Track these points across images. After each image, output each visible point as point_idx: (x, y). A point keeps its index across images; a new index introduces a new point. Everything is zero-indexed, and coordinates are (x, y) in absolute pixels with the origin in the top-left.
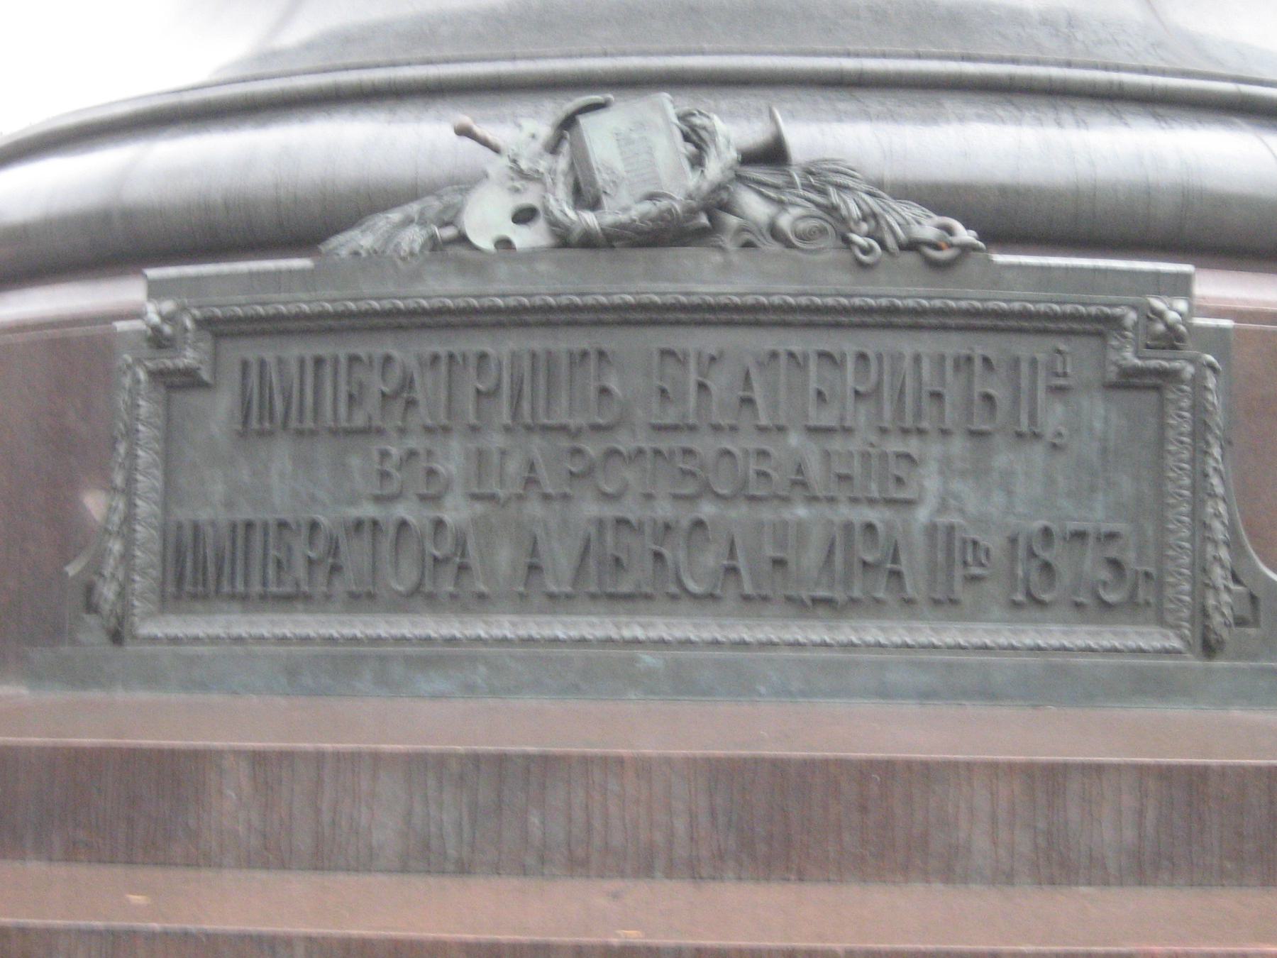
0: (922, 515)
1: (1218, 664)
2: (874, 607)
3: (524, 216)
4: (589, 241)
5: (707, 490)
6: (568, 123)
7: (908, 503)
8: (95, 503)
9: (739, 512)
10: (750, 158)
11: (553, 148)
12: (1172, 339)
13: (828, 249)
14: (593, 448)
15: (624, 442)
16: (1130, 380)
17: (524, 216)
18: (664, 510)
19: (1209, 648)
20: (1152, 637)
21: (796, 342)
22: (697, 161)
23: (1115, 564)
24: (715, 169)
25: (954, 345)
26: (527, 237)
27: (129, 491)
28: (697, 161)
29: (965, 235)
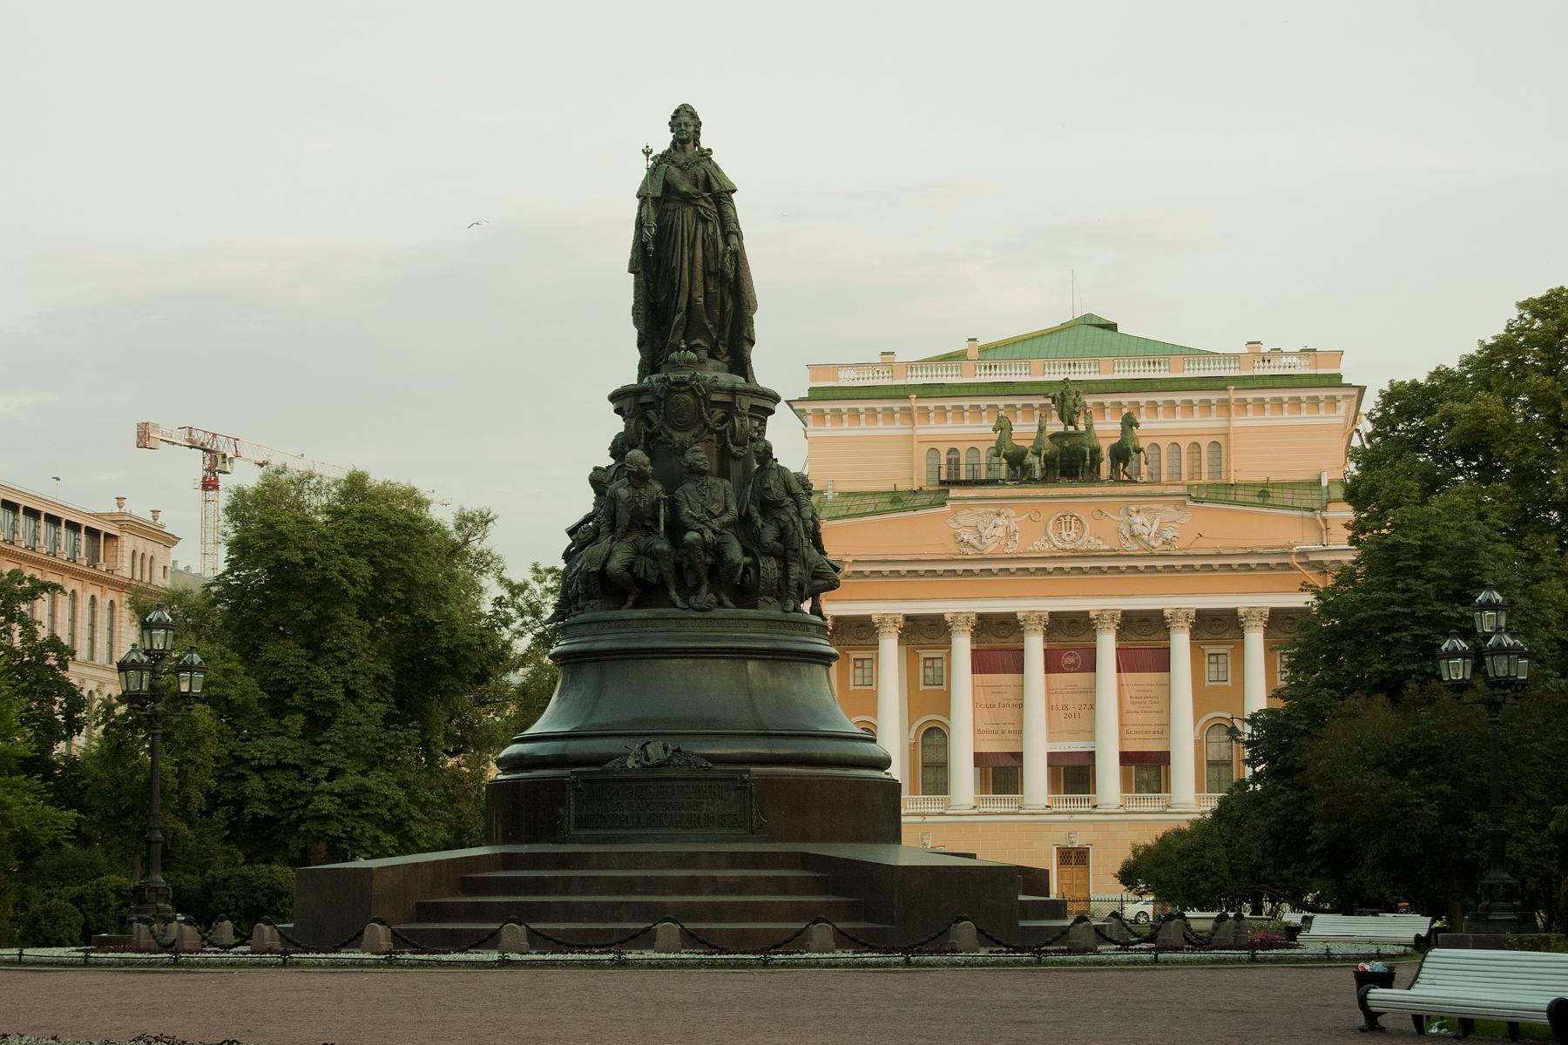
0: (704, 812)
1: (755, 836)
2: (696, 827)
3: (637, 762)
4: (647, 767)
5: (667, 808)
6: (644, 745)
7: (701, 810)
8: (561, 811)
9: (674, 812)
10: (674, 751)
11: (642, 749)
12: (746, 781)
13: (687, 768)
14: (649, 802)
15: (654, 801)
16: (738, 788)
17: (637, 762)
18: (661, 812)
19: (753, 833)
20: (741, 831)
21: (683, 784)
22: (666, 753)
23: (736, 819)
24: (668, 755)
25: (709, 783)
26: (637, 766)
27: (569, 808)
28: (666, 753)
29: (710, 765)
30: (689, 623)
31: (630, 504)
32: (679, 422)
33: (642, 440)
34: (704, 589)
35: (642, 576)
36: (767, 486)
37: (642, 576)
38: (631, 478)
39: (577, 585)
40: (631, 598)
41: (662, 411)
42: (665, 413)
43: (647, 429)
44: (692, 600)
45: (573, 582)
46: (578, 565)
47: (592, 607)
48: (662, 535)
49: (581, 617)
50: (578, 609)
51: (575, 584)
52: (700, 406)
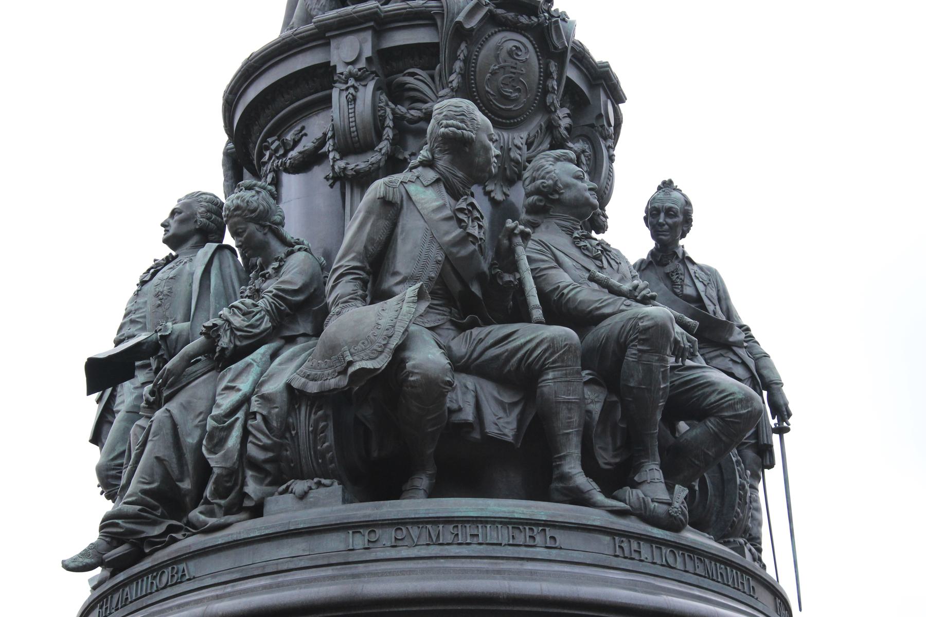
30: (646, 551)
31: (445, 226)
32: (507, 99)
33: (389, 133)
34: (653, 472)
35: (468, 415)
36: (689, 291)
37: (468, 415)
38: (443, 162)
39: (246, 433)
40: (423, 482)
41: (458, 65)
42: (465, 75)
43: (402, 109)
44: (633, 495)
45: (231, 426)
46: (245, 385)
47: (303, 496)
48: (538, 313)
49: (244, 528)
50: (236, 507)
51: (236, 433)
52: (547, 75)
